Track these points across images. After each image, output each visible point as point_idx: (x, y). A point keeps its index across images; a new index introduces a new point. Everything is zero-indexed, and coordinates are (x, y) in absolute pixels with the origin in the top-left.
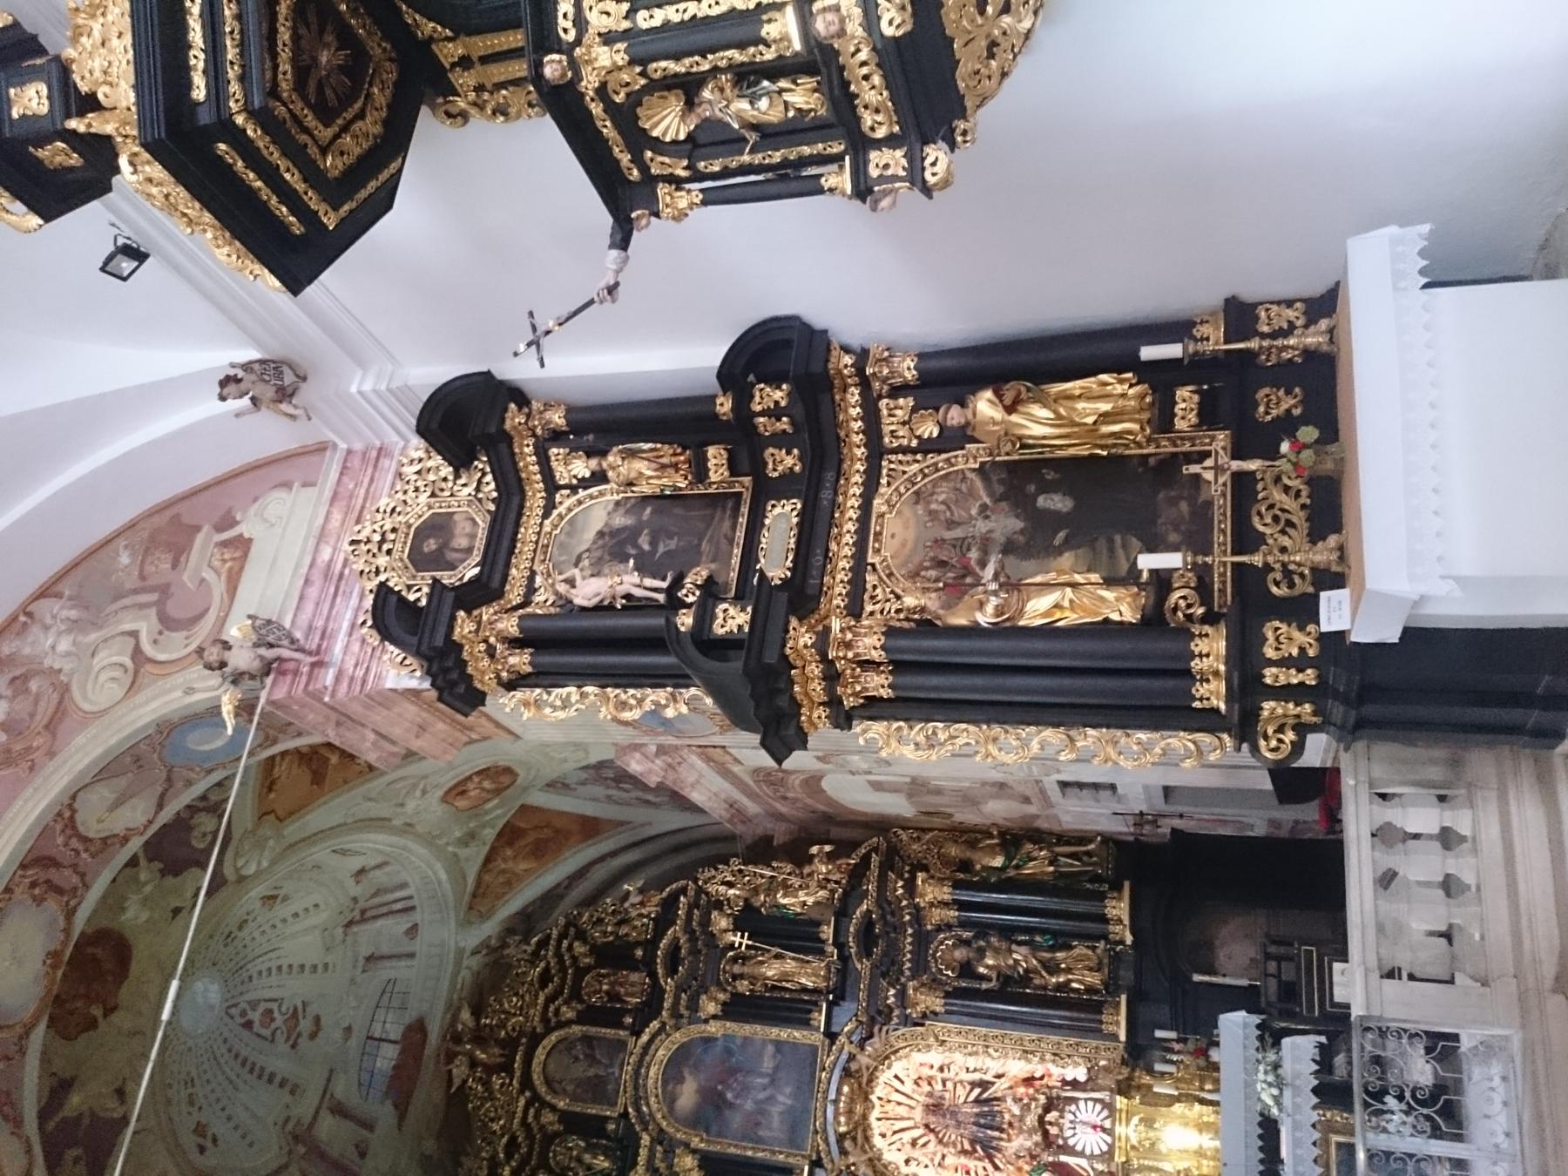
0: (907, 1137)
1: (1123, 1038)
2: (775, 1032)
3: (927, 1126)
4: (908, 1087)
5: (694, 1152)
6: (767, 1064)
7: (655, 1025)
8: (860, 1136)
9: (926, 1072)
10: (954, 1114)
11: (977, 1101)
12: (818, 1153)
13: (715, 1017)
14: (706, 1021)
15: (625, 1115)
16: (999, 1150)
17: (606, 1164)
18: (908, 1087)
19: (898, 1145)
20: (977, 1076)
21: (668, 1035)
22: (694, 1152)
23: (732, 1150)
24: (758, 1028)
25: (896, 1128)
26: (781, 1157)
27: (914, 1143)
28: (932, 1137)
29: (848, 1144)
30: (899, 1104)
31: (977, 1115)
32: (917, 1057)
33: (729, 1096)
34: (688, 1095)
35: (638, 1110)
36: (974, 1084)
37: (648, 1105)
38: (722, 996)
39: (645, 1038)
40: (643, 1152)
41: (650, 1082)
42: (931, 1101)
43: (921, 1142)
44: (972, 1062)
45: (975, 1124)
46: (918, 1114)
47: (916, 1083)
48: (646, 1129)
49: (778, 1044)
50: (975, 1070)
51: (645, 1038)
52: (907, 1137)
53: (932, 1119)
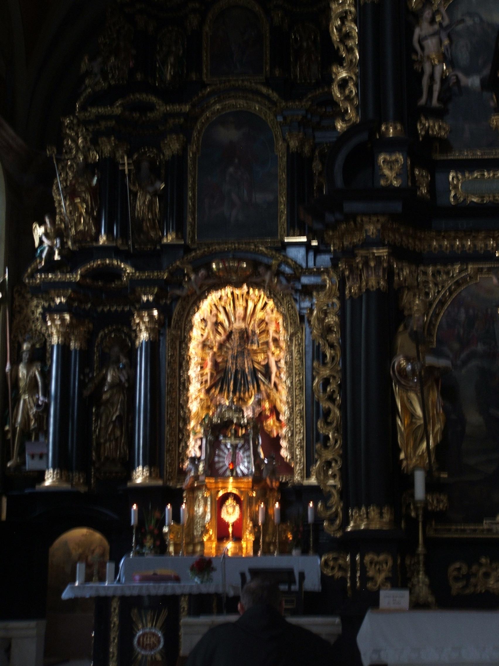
0: (222, 317)
1: (306, 482)
2: (283, 199)
3: (231, 333)
4: (259, 315)
5: (184, 149)
6: (259, 197)
7: (275, 96)
8: (211, 281)
9: (272, 328)
10: (241, 353)
11: (254, 372)
12: (195, 250)
13: (288, 146)
14: (284, 140)
15: (204, 86)
16: (221, 391)
17: (168, 77)
18: (259, 315)
19: (214, 311)
20: (274, 369)
21: (269, 108)
22: (184, 149)
23: (190, 180)
24: (285, 186)
25: (228, 308)
26: (190, 219)
27: (217, 324)
28: (223, 337)
29: (202, 272)
30: (246, 309)
31: (243, 372)
32: (280, 321)
33: (231, 170)
34: (228, 134)
35: (210, 95)
36: (267, 367)
37: (215, 103)
38: (307, 149)
39: (264, 90)
40: (177, 108)
41: (233, 102)
42: (250, 332)
43: (220, 329)
44: (282, 364)
45: (237, 371)
46: (239, 325)
47: (262, 321)
48: (193, 106)
49: (275, 203)
50: (278, 368)
51: (264, 90)
52: (222, 317)
53: (236, 337)
